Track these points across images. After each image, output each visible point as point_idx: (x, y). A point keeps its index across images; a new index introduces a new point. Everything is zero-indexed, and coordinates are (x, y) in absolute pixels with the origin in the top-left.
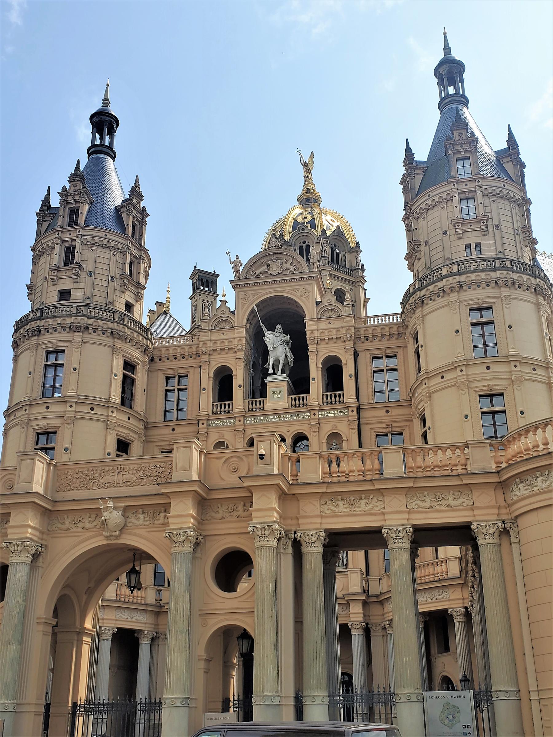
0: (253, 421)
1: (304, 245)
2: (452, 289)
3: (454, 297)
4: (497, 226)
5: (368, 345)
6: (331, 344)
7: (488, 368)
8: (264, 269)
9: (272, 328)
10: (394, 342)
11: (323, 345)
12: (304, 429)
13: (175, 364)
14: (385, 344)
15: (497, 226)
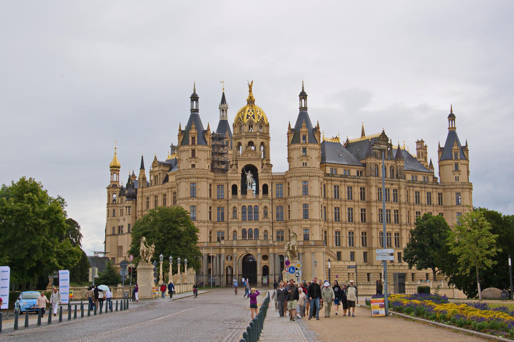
0: (244, 201)
1: (251, 125)
2: (299, 177)
3: (299, 178)
4: (311, 158)
5: (275, 181)
6: (265, 181)
7: (306, 198)
8: (246, 155)
9: (247, 172)
10: (282, 181)
11: (263, 181)
12: (257, 204)
13: (220, 182)
14: (280, 181)
15: (311, 158)
